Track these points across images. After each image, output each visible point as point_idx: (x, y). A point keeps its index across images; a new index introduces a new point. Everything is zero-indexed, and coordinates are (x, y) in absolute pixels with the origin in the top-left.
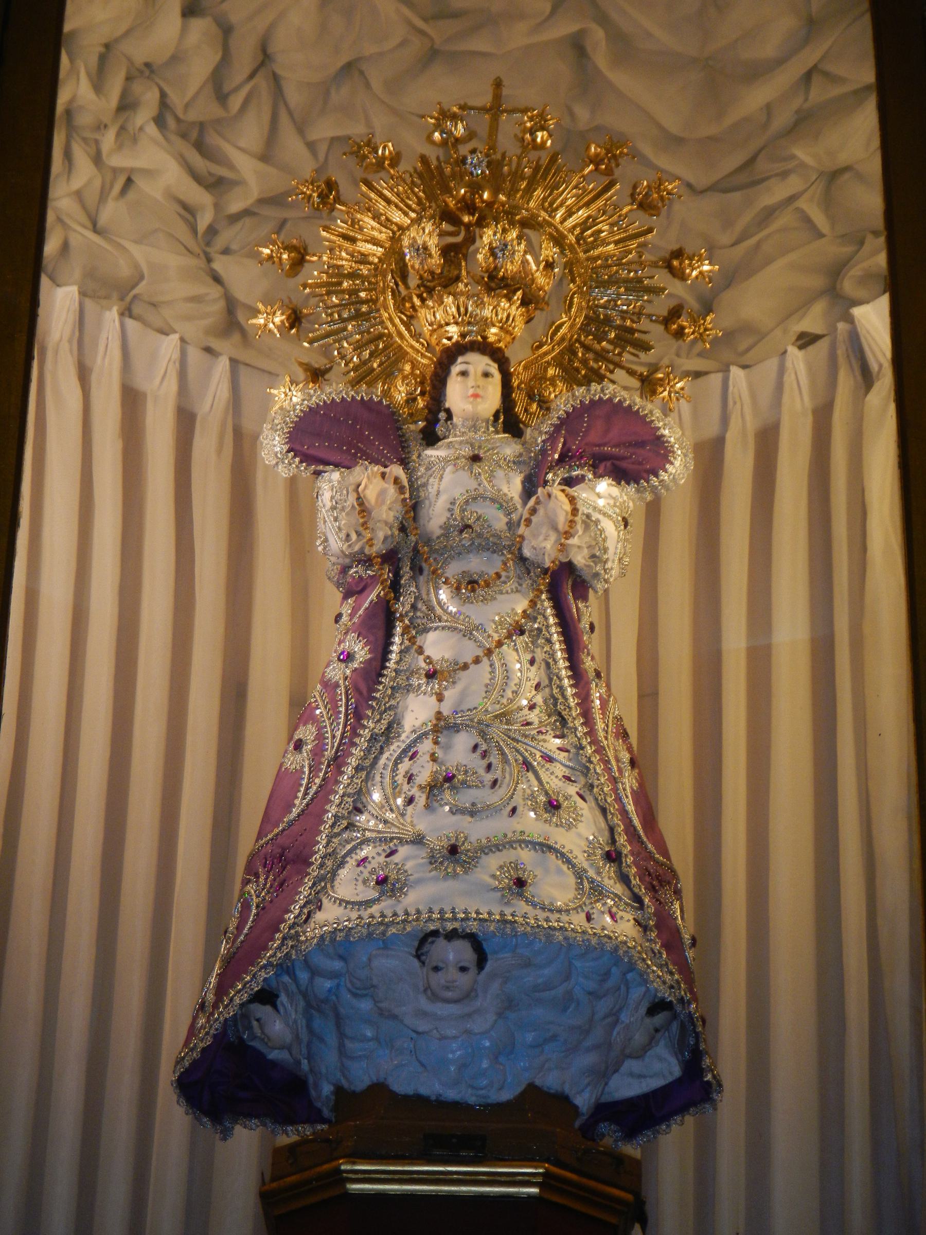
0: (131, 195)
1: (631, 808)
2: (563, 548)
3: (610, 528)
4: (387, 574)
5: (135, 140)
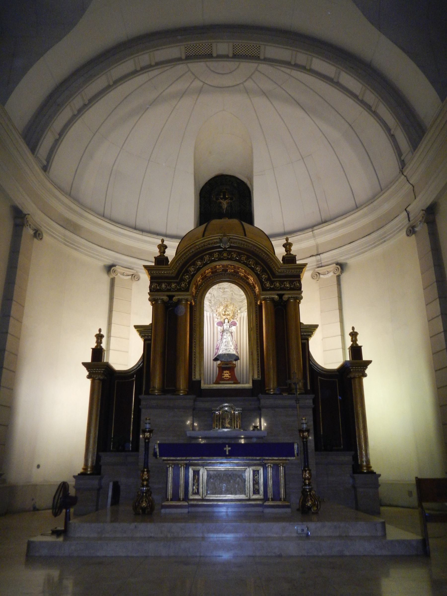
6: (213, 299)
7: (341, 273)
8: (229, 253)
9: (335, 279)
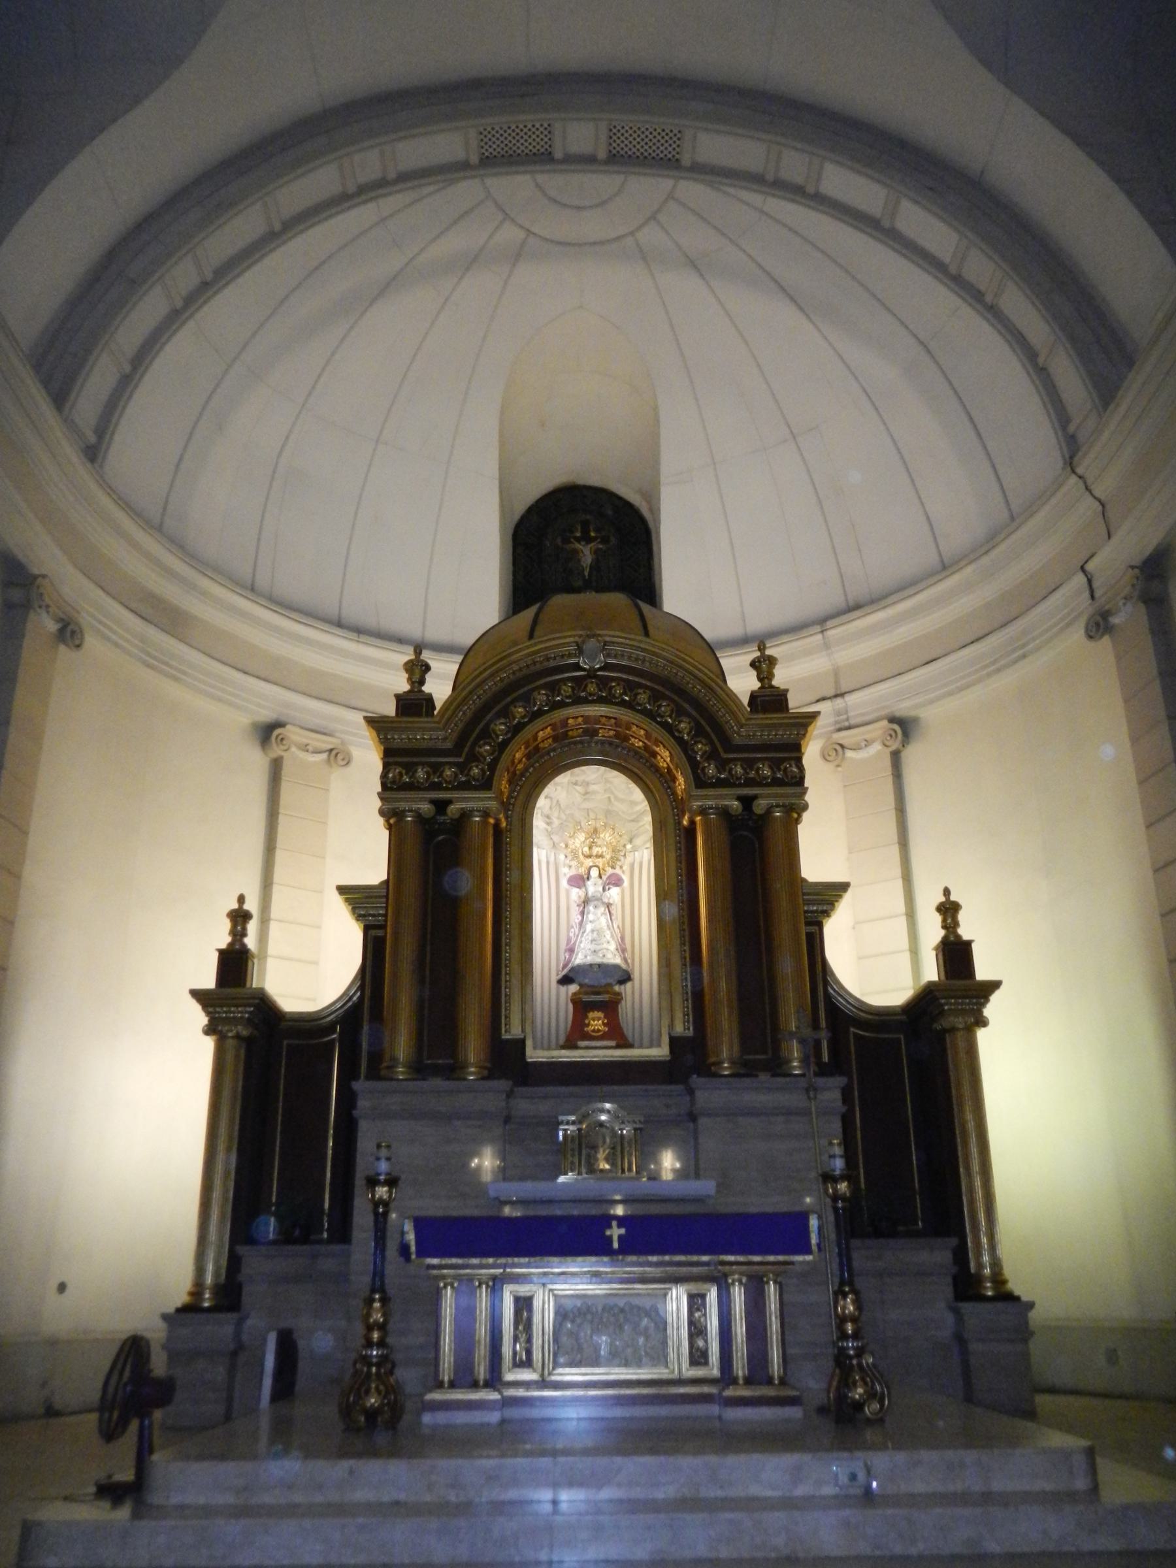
6: (556, 814)
7: (903, 746)
8: (604, 683)
9: (887, 762)
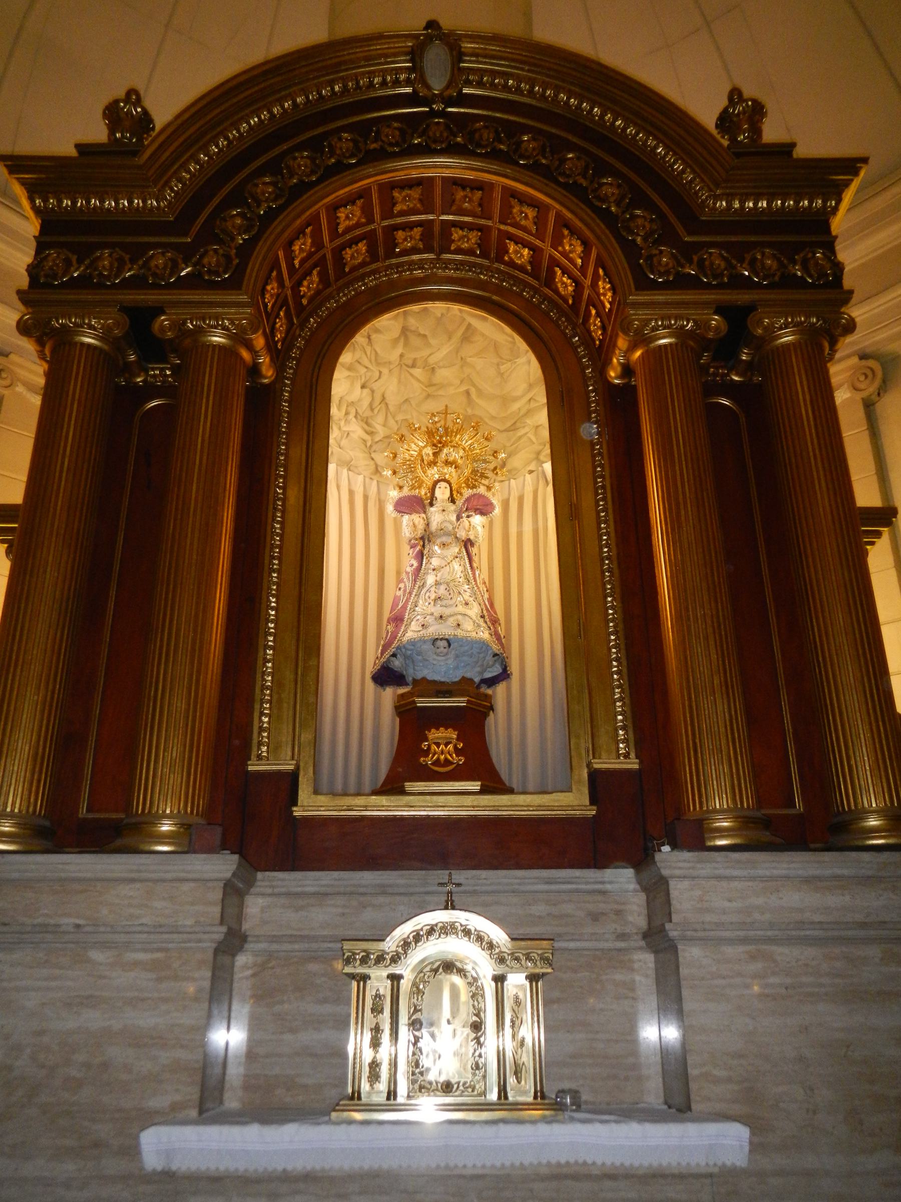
0: (349, 438)
1: (487, 603)
2: (467, 535)
3: (479, 529)
4: (421, 543)
5: (349, 423)
6: (380, 419)
7: (879, 394)
